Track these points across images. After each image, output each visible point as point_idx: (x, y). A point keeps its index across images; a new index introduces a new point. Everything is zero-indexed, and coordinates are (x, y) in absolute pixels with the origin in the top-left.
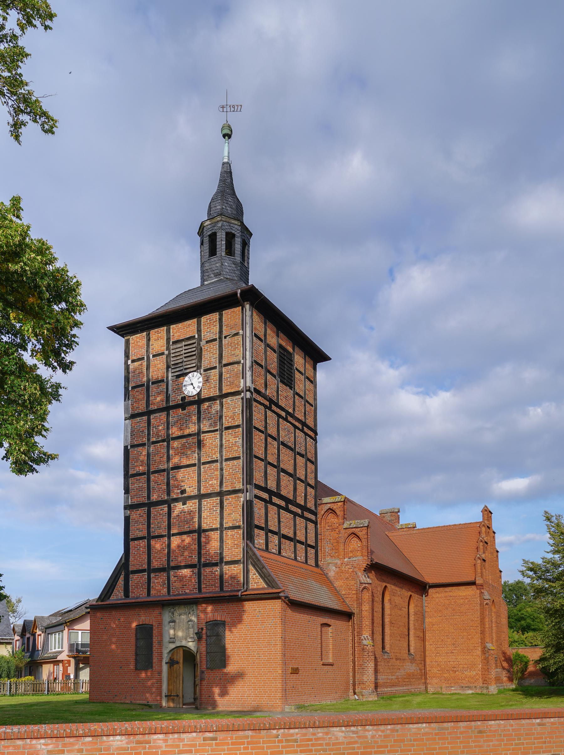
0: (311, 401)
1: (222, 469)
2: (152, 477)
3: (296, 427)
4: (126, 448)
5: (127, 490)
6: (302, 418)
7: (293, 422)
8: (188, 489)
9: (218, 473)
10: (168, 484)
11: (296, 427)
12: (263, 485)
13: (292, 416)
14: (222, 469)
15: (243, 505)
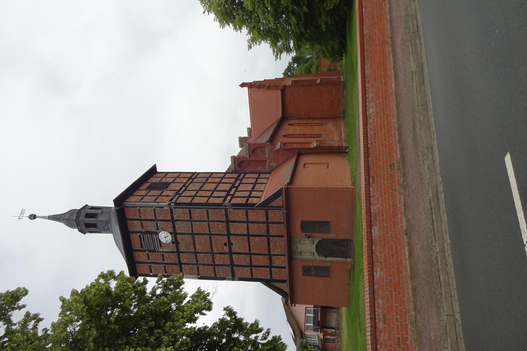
0: (178, 174)
1: (213, 221)
2: (216, 263)
3: (192, 182)
4: (199, 278)
5: (223, 279)
6: (187, 179)
7: (188, 183)
8: (224, 242)
9: (215, 223)
10: (221, 253)
11: (192, 182)
12: (223, 198)
13: (185, 184)
14: (213, 221)
15: (234, 209)
